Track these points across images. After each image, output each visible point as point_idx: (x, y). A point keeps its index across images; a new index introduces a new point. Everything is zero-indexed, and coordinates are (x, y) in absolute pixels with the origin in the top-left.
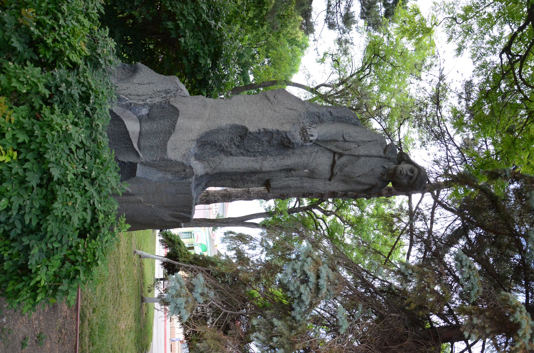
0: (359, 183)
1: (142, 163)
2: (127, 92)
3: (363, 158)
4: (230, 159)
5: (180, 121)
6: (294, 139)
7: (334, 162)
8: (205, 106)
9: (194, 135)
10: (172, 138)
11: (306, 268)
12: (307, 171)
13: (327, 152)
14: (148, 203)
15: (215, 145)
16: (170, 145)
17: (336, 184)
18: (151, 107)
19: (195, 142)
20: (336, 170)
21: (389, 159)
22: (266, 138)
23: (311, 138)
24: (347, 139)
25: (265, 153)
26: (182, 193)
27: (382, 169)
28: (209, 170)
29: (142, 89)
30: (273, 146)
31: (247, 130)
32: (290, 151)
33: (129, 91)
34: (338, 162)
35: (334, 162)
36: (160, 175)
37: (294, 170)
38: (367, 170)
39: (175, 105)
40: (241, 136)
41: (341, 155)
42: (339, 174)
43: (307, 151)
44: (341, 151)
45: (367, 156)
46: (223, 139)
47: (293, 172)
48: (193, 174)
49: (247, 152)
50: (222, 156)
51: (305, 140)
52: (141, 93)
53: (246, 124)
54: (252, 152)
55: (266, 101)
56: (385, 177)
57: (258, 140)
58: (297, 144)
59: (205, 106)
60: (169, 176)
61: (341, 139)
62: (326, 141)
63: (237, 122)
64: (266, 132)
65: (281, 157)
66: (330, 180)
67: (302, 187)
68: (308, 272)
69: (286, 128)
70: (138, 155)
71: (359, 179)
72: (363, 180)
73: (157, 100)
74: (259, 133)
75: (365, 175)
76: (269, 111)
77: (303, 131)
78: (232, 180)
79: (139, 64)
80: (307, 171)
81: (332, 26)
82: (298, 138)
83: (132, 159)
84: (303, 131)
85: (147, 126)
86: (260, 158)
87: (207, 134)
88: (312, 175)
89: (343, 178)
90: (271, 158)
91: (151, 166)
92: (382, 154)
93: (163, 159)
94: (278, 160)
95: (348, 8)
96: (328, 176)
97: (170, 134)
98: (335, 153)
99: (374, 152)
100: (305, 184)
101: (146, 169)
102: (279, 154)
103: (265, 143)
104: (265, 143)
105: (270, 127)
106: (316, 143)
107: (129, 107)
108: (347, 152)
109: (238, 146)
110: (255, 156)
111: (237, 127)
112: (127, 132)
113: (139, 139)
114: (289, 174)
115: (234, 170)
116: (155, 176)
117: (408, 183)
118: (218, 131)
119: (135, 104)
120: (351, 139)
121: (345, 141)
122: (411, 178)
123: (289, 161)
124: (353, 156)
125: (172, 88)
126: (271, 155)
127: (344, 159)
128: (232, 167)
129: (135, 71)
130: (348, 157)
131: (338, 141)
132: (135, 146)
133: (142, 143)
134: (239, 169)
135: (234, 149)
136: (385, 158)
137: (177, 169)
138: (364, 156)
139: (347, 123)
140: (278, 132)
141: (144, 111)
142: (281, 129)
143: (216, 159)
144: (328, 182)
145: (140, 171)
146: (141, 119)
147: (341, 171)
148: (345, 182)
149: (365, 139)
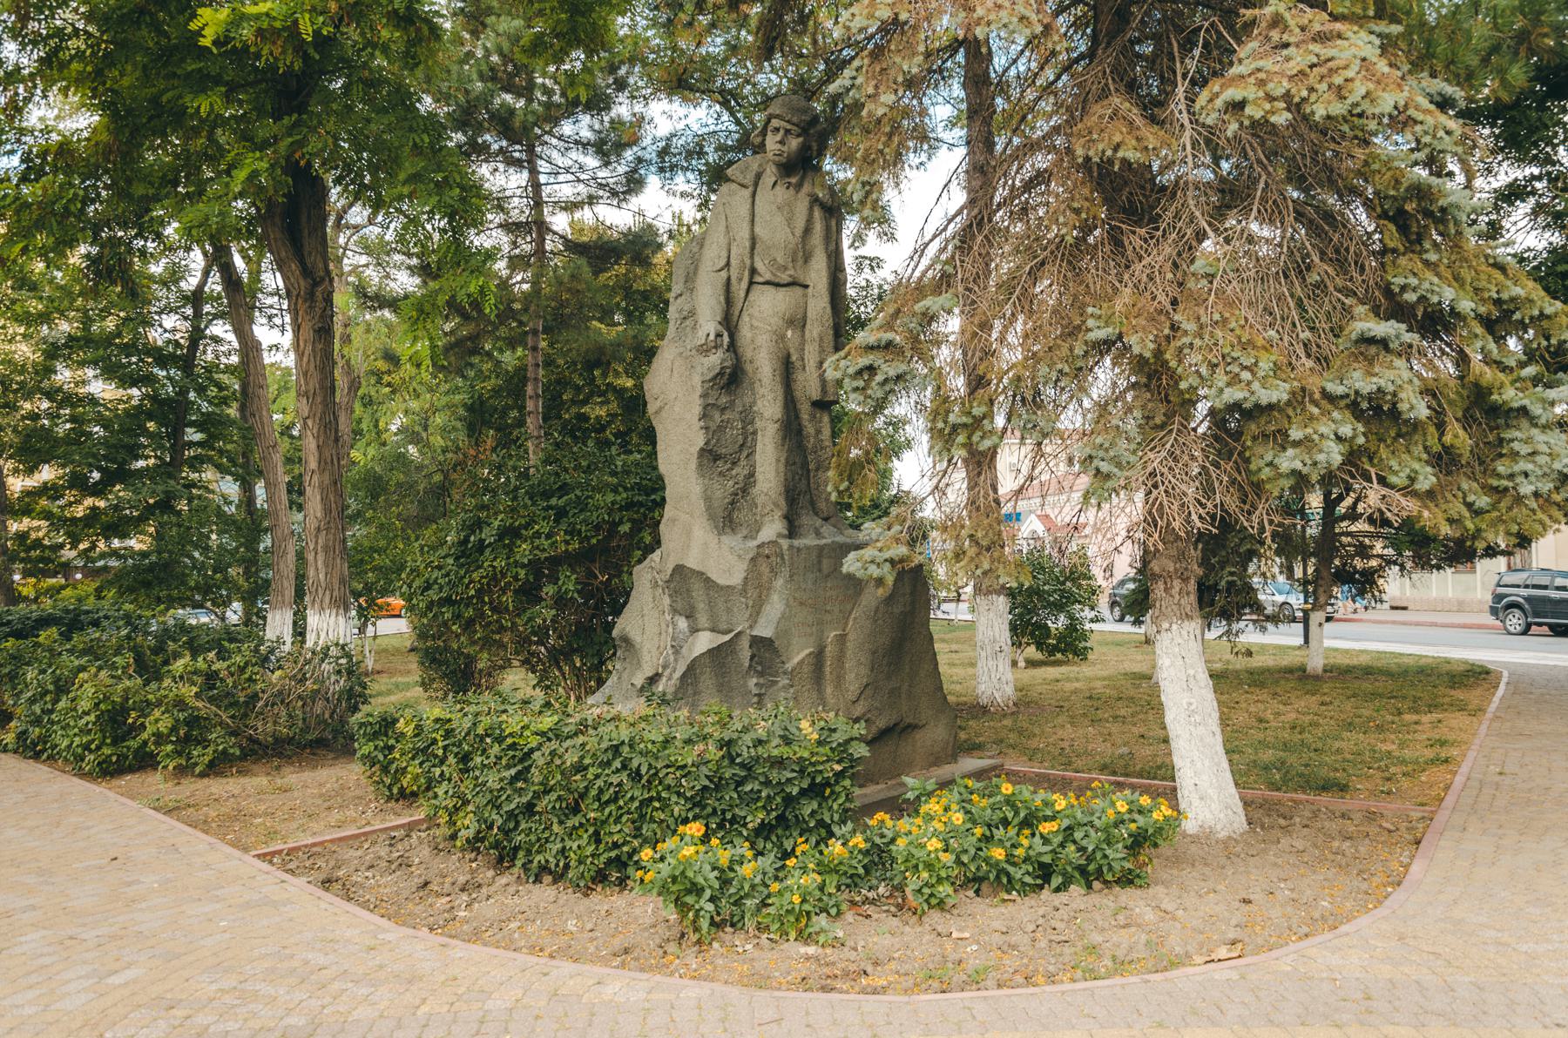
0: (807, 231)
1: (751, 627)
2: (655, 653)
3: (757, 230)
4: (759, 476)
5: (692, 563)
6: (713, 367)
7: (767, 283)
8: (674, 520)
9: (712, 539)
10: (714, 577)
11: (851, 371)
12: (789, 333)
13: (751, 297)
14: (846, 624)
15: (732, 503)
16: (722, 581)
17: (813, 275)
18: (675, 611)
19: (724, 538)
20: (785, 278)
21: (758, 176)
22: (717, 417)
23: (712, 337)
24: (723, 262)
25: (748, 417)
26: (820, 562)
27: (778, 188)
28: (778, 514)
29: (651, 629)
30: (732, 402)
31: (702, 450)
32: (748, 368)
33: (654, 650)
34: (768, 276)
35: (767, 283)
36: (775, 597)
37: (789, 356)
38: (779, 219)
39: (669, 572)
40: (715, 460)
41: (753, 271)
42: (791, 272)
43: (749, 335)
44: (746, 273)
45: (753, 221)
46: (722, 490)
47: (794, 358)
48: (773, 543)
49: (746, 445)
50: (755, 491)
51: (716, 347)
52: (656, 630)
53: (695, 450)
54: (745, 439)
55: (663, 414)
56: (794, 180)
57: (721, 428)
58: (723, 360)
59: (674, 520)
60: (779, 583)
61: (724, 274)
62: (729, 301)
63: (693, 464)
64: (704, 416)
65: (757, 385)
66: (806, 287)
67: (821, 339)
68: (860, 366)
69: (697, 380)
70: (739, 633)
71: (799, 232)
72: (800, 224)
73: (667, 601)
74: (707, 428)
75: (789, 221)
76: (677, 409)
77: (704, 350)
78: (817, 470)
79: (615, 633)
80: (789, 333)
81: (634, 183)
82: (715, 360)
83: (745, 643)
84: (704, 350)
85: (703, 620)
86: (759, 424)
87: (712, 517)
88: (798, 322)
89: (800, 262)
90: (759, 403)
91: (758, 613)
92: (747, 193)
93: (744, 591)
94: (762, 391)
95: (583, 145)
96: (798, 291)
97: (708, 580)
98: (751, 283)
99: (744, 210)
100: (815, 334)
101: (762, 620)
102: (753, 389)
103: (725, 417)
104: (725, 417)
105: (697, 410)
106: (729, 322)
107: (677, 650)
108: (748, 262)
109: (734, 463)
110: (755, 433)
111: (700, 465)
112: (710, 651)
113: (719, 632)
114: (798, 364)
115: (782, 468)
116: (775, 607)
117: (798, 136)
118: (708, 499)
119: (673, 639)
120: (724, 254)
121: (728, 264)
122: (787, 131)
123: (763, 366)
124: (753, 248)
125: (649, 577)
126: (755, 403)
127: (759, 265)
128: (773, 474)
129: (626, 640)
130: (757, 259)
131: (729, 279)
132: (727, 638)
133: (724, 626)
134: (778, 461)
135: (740, 471)
136: (756, 185)
137: (764, 568)
138: (752, 230)
139: (699, 260)
140: (704, 396)
141: (683, 624)
142: (699, 391)
143: (759, 501)
144: (810, 290)
145: (765, 630)
146: (694, 630)
147: (786, 268)
148: (807, 258)
149: (722, 228)
